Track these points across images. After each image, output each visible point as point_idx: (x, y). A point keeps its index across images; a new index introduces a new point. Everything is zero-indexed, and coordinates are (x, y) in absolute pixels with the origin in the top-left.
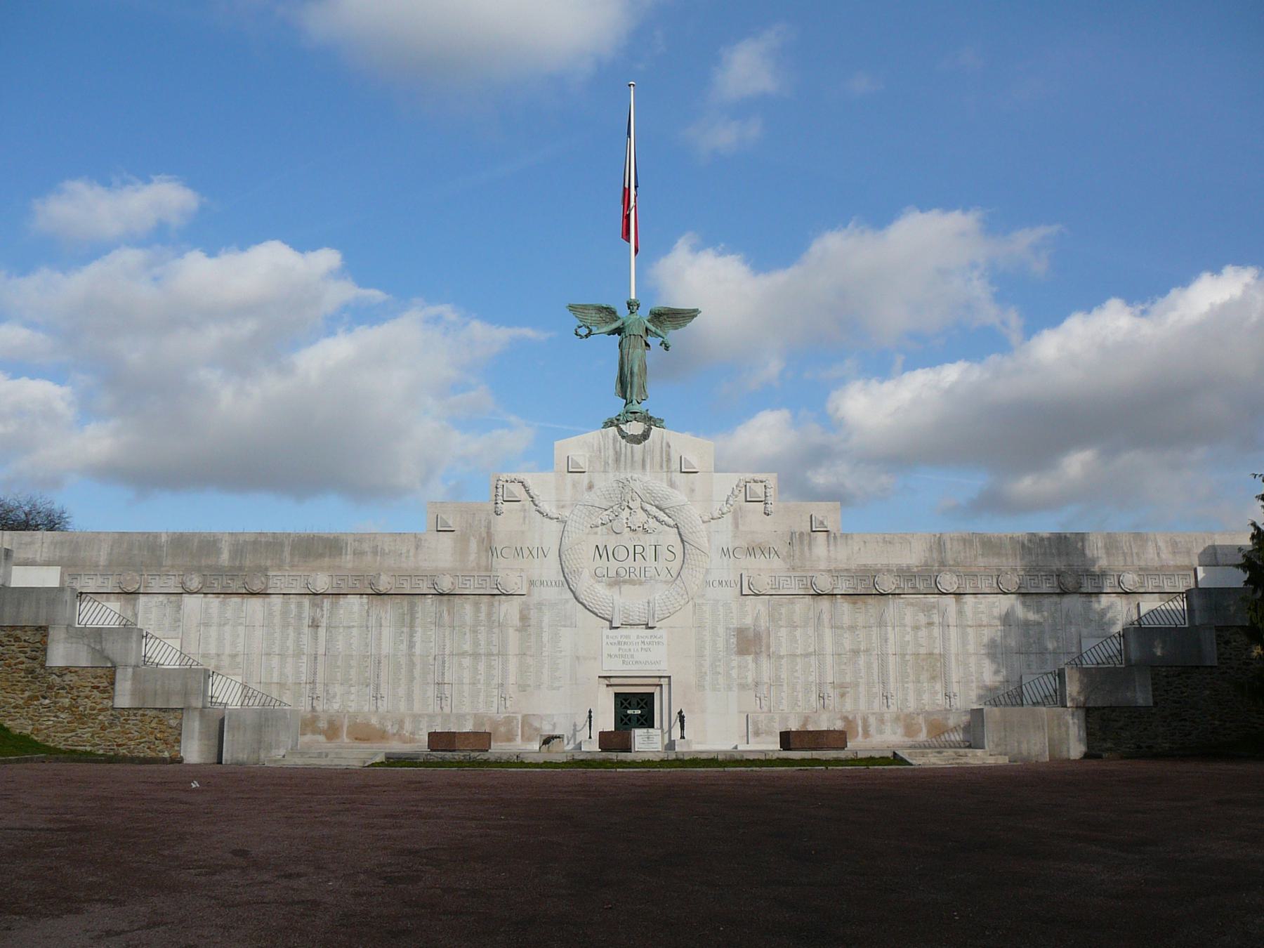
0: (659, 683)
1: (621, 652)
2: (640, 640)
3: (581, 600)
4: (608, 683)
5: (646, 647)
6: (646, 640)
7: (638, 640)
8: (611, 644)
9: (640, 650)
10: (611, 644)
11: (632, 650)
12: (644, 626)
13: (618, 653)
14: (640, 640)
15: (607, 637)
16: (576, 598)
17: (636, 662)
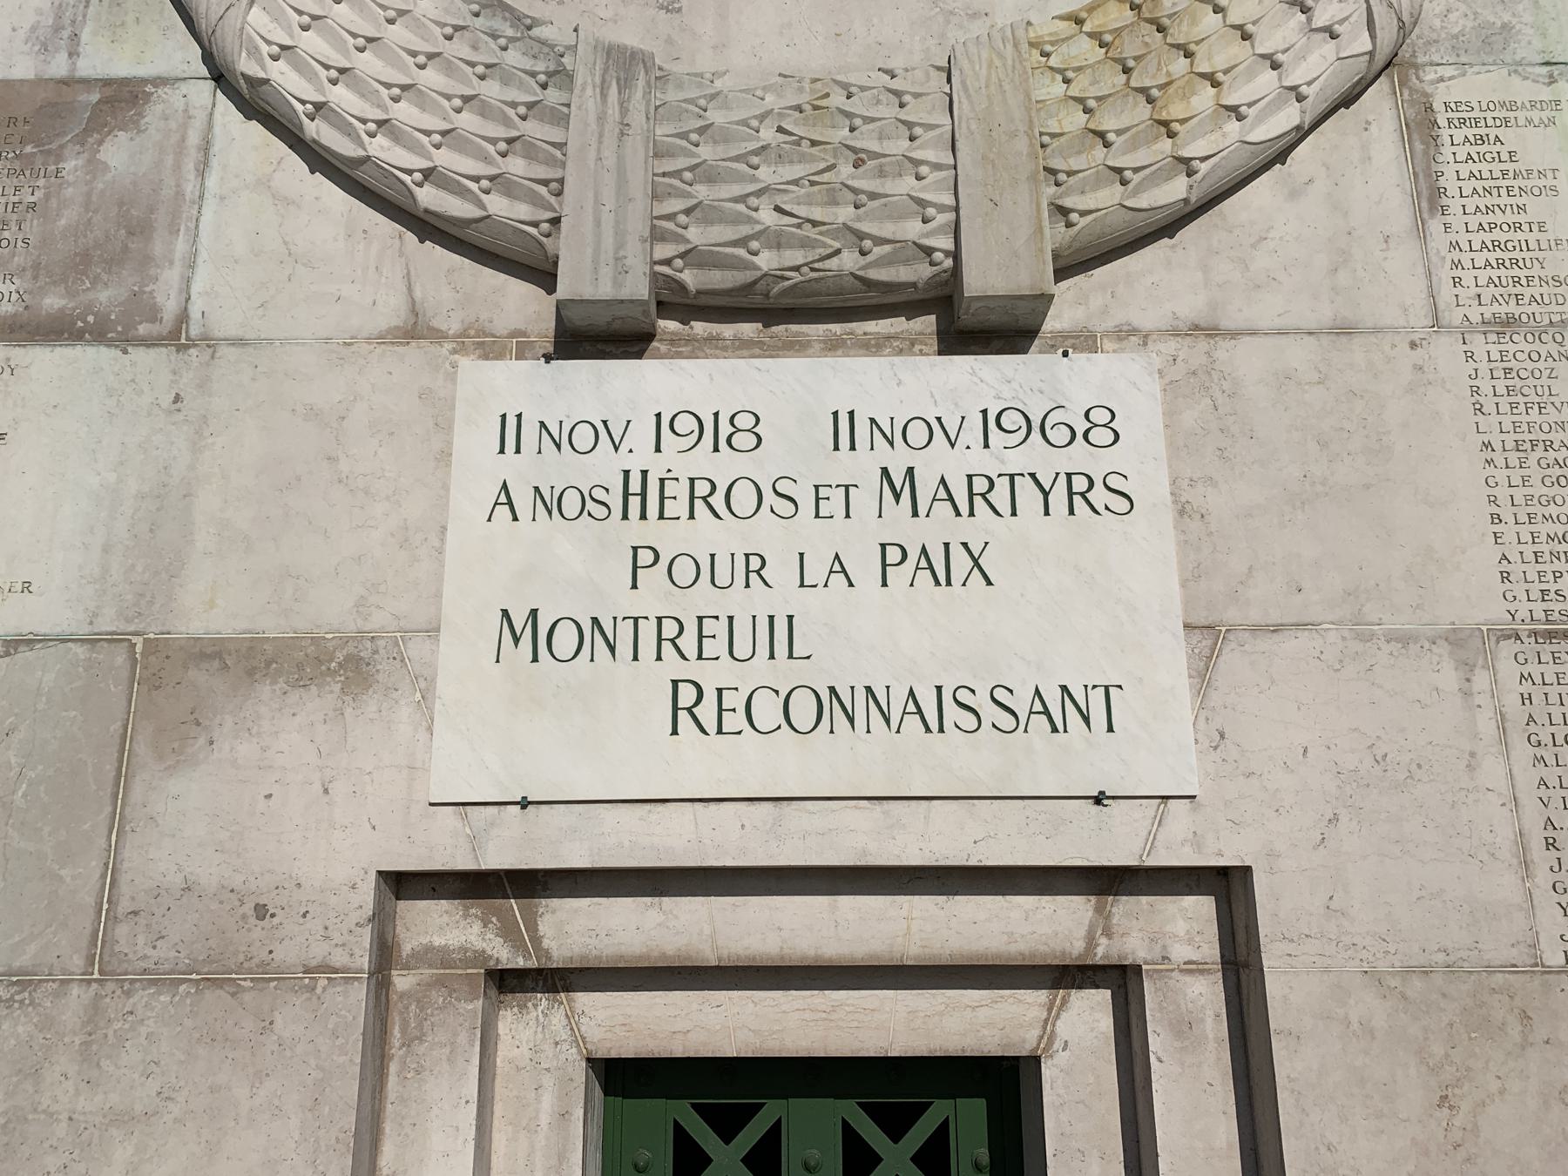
0: (1103, 952)
1: (653, 598)
2: (863, 466)
3: (246, 65)
4: (505, 956)
5: (937, 528)
6: (936, 463)
7: (846, 465)
8: (548, 503)
9: (865, 567)
10: (548, 503)
11: (781, 571)
12: (927, 323)
13: (618, 601)
14: (863, 466)
15: (510, 433)
16: (220, 77)
17: (832, 703)
